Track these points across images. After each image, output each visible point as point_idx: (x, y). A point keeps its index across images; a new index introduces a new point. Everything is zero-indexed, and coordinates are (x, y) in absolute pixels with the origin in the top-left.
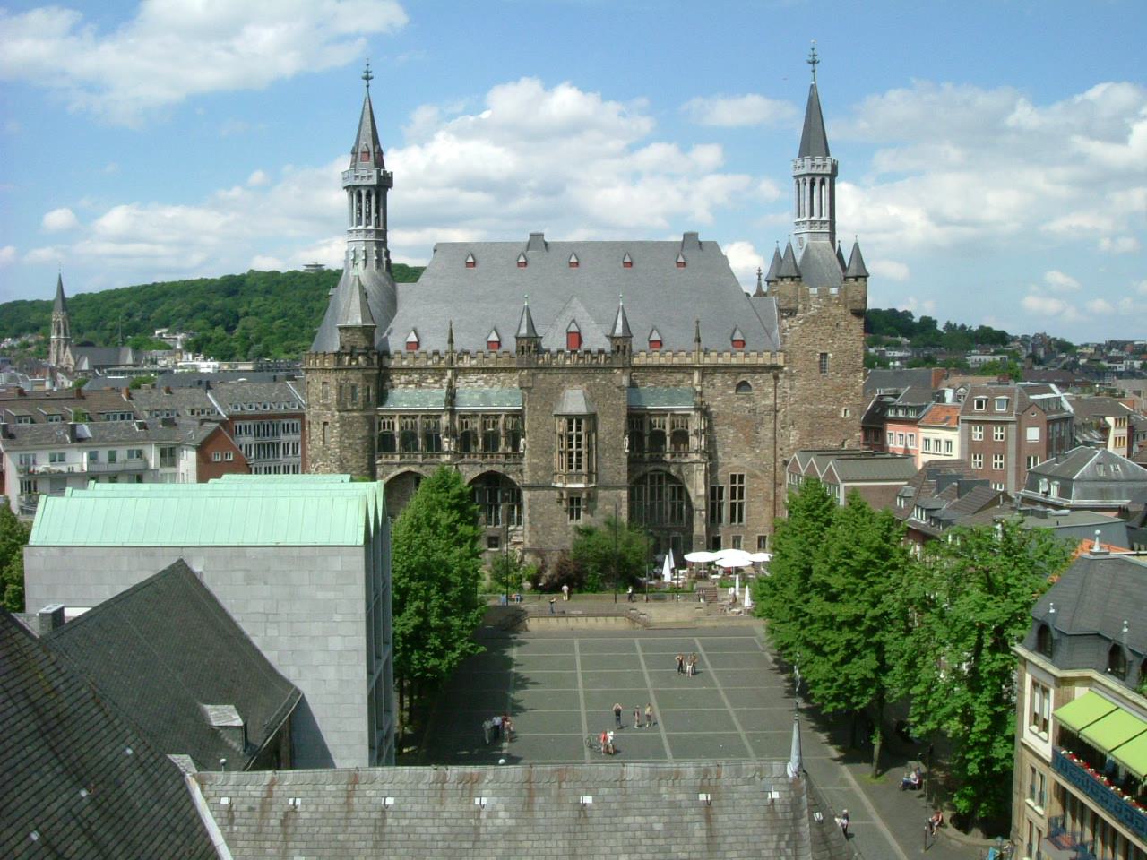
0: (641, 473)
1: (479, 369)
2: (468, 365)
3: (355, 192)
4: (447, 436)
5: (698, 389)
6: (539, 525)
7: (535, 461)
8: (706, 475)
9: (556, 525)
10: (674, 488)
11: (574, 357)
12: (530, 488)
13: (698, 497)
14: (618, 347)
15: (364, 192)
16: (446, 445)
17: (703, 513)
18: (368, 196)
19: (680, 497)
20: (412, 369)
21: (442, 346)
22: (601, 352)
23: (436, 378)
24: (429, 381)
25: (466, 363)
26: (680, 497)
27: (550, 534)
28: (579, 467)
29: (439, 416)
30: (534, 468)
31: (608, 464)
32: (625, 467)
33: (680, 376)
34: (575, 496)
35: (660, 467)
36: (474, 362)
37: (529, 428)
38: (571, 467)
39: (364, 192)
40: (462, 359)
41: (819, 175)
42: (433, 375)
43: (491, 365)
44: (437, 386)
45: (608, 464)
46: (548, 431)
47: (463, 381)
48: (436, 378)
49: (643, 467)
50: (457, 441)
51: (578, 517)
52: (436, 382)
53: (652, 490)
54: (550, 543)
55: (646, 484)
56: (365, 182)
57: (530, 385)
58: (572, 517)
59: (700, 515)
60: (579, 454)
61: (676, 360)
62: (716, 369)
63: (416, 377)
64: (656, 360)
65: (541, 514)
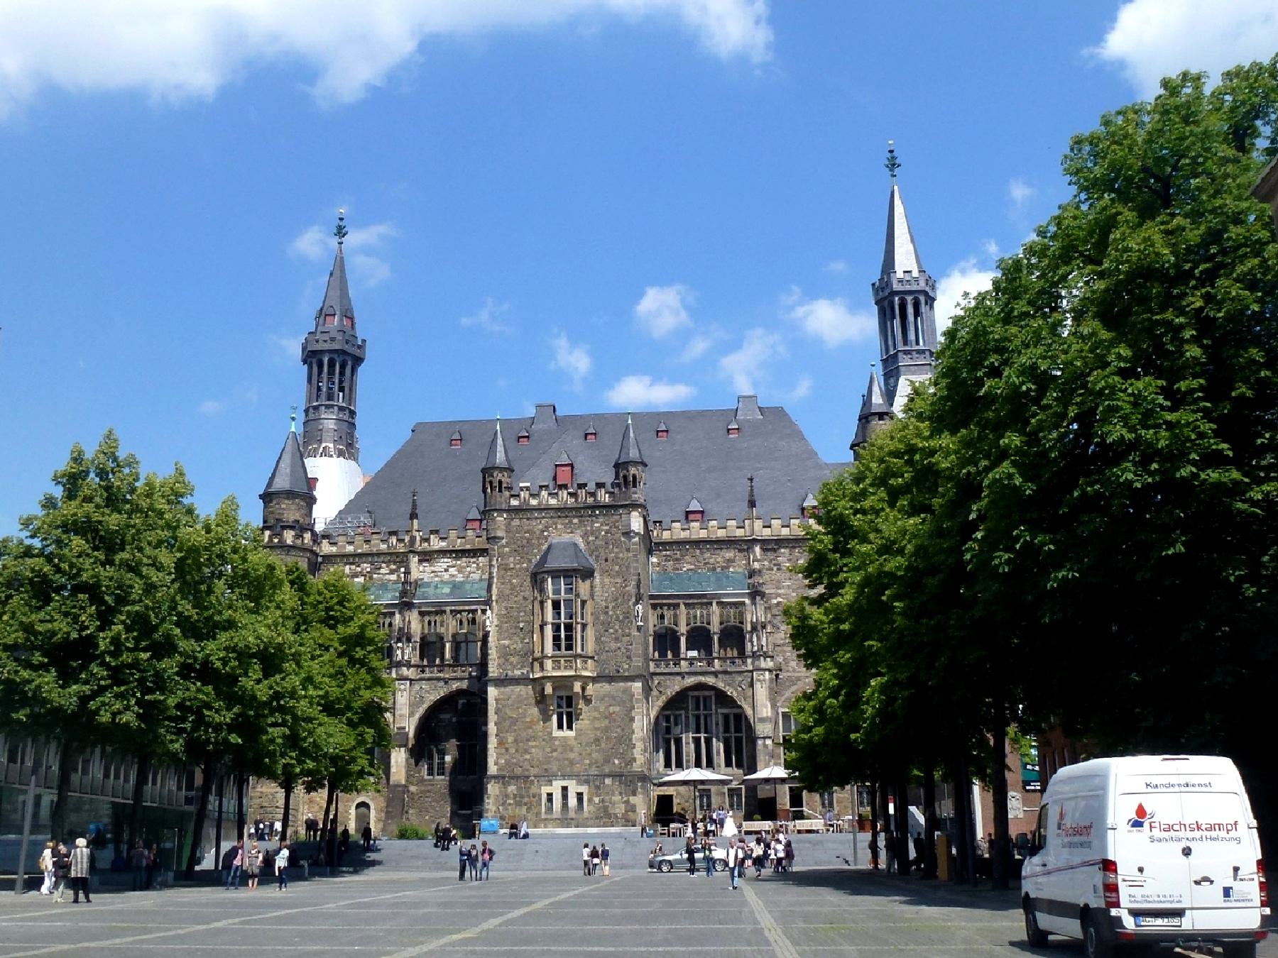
0: (677, 688)
1: (451, 552)
2: (436, 548)
3: (314, 361)
4: (399, 640)
5: (756, 565)
6: (510, 739)
7: (506, 642)
8: (771, 689)
9: (534, 738)
10: (726, 717)
11: (564, 494)
12: (501, 682)
13: (762, 720)
14: (625, 477)
15: (326, 360)
16: (399, 652)
17: (769, 742)
18: (332, 364)
19: (738, 730)
20: (360, 555)
21: (401, 523)
22: (600, 485)
23: (393, 567)
24: (382, 571)
25: (436, 544)
26: (738, 730)
27: (526, 751)
28: (569, 647)
29: (393, 614)
30: (505, 654)
31: (613, 645)
32: (637, 649)
33: (729, 554)
34: (564, 693)
35: (702, 679)
36: (443, 544)
37: (500, 595)
38: (557, 646)
39: (326, 360)
40: (427, 540)
41: (910, 292)
42: (388, 563)
43: (468, 547)
44: (394, 577)
45: (613, 645)
46: (525, 598)
47: (428, 569)
48: (393, 567)
49: (679, 678)
50: (414, 649)
51: (570, 727)
52: (392, 572)
53: (698, 718)
54: (526, 765)
55: (686, 709)
56: (326, 346)
57: (500, 534)
58: (560, 726)
59: (765, 746)
60: (569, 628)
61: (721, 534)
62: (780, 543)
63: (366, 567)
64: (696, 531)
65: (514, 722)
